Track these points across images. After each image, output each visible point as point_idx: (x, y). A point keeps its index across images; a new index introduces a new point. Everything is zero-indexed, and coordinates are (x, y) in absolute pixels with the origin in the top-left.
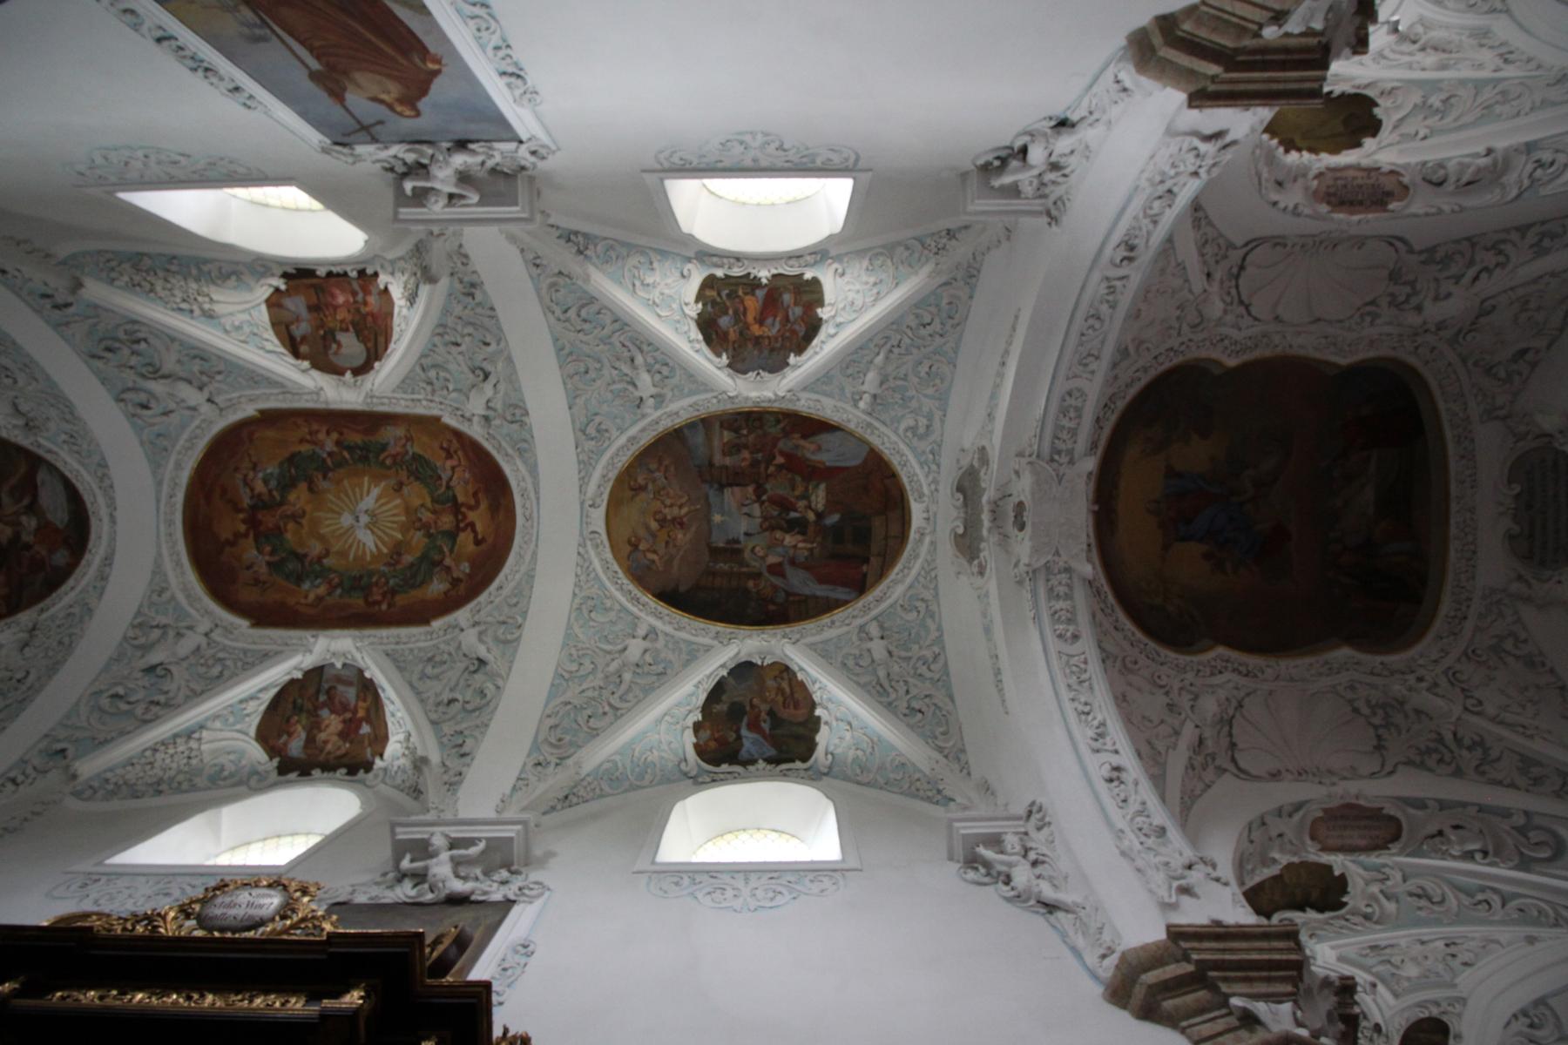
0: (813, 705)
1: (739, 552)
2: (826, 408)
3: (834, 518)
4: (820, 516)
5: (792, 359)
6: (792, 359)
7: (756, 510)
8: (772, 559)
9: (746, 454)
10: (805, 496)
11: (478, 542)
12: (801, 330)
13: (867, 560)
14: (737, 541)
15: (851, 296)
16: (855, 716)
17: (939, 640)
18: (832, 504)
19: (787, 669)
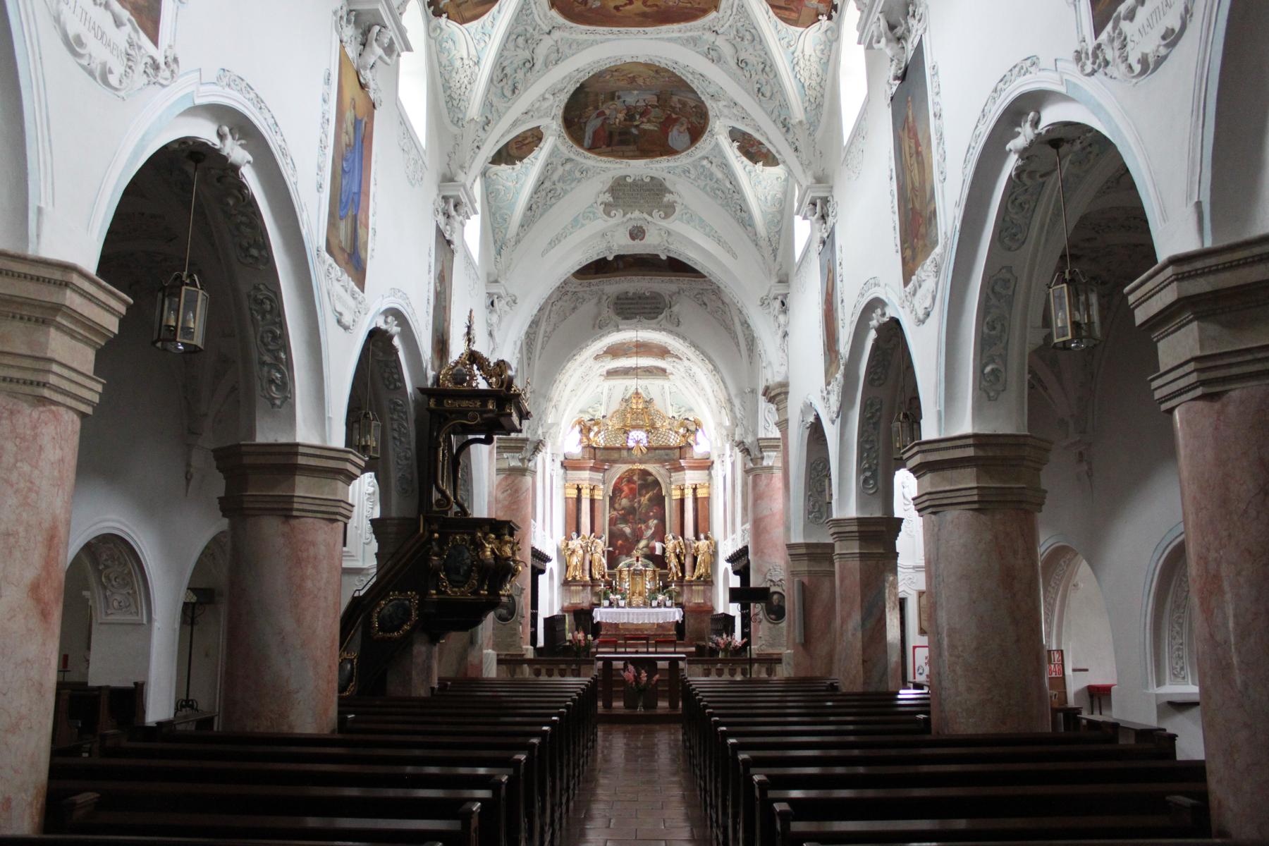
0: (521, 159)
1: (613, 99)
2: (704, 145)
3: (634, 131)
4: (637, 126)
5: (736, 144)
6: (736, 144)
7: (641, 103)
8: (607, 112)
9: (678, 106)
10: (649, 121)
11: (617, 8)
12: (753, 150)
13: (608, 146)
14: (619, 98)
15: (764, 183)
16: (522, 186)
17: (566, 192)
18: (645, 131)
19: (540, 140)
